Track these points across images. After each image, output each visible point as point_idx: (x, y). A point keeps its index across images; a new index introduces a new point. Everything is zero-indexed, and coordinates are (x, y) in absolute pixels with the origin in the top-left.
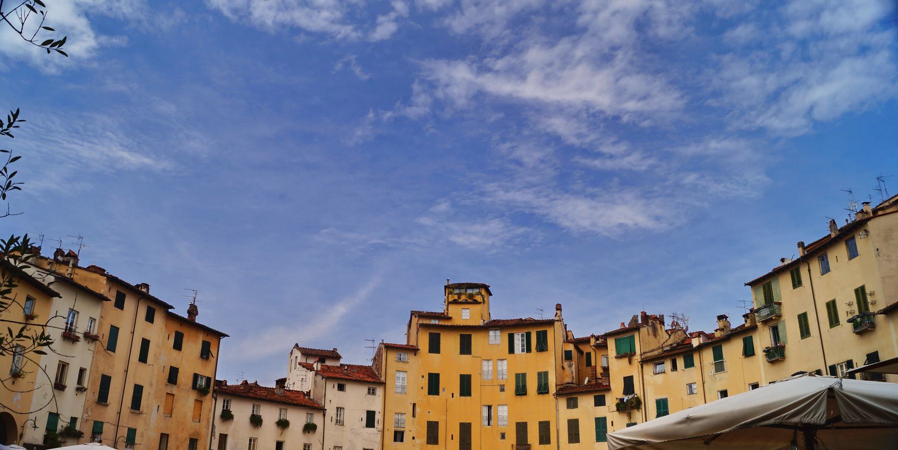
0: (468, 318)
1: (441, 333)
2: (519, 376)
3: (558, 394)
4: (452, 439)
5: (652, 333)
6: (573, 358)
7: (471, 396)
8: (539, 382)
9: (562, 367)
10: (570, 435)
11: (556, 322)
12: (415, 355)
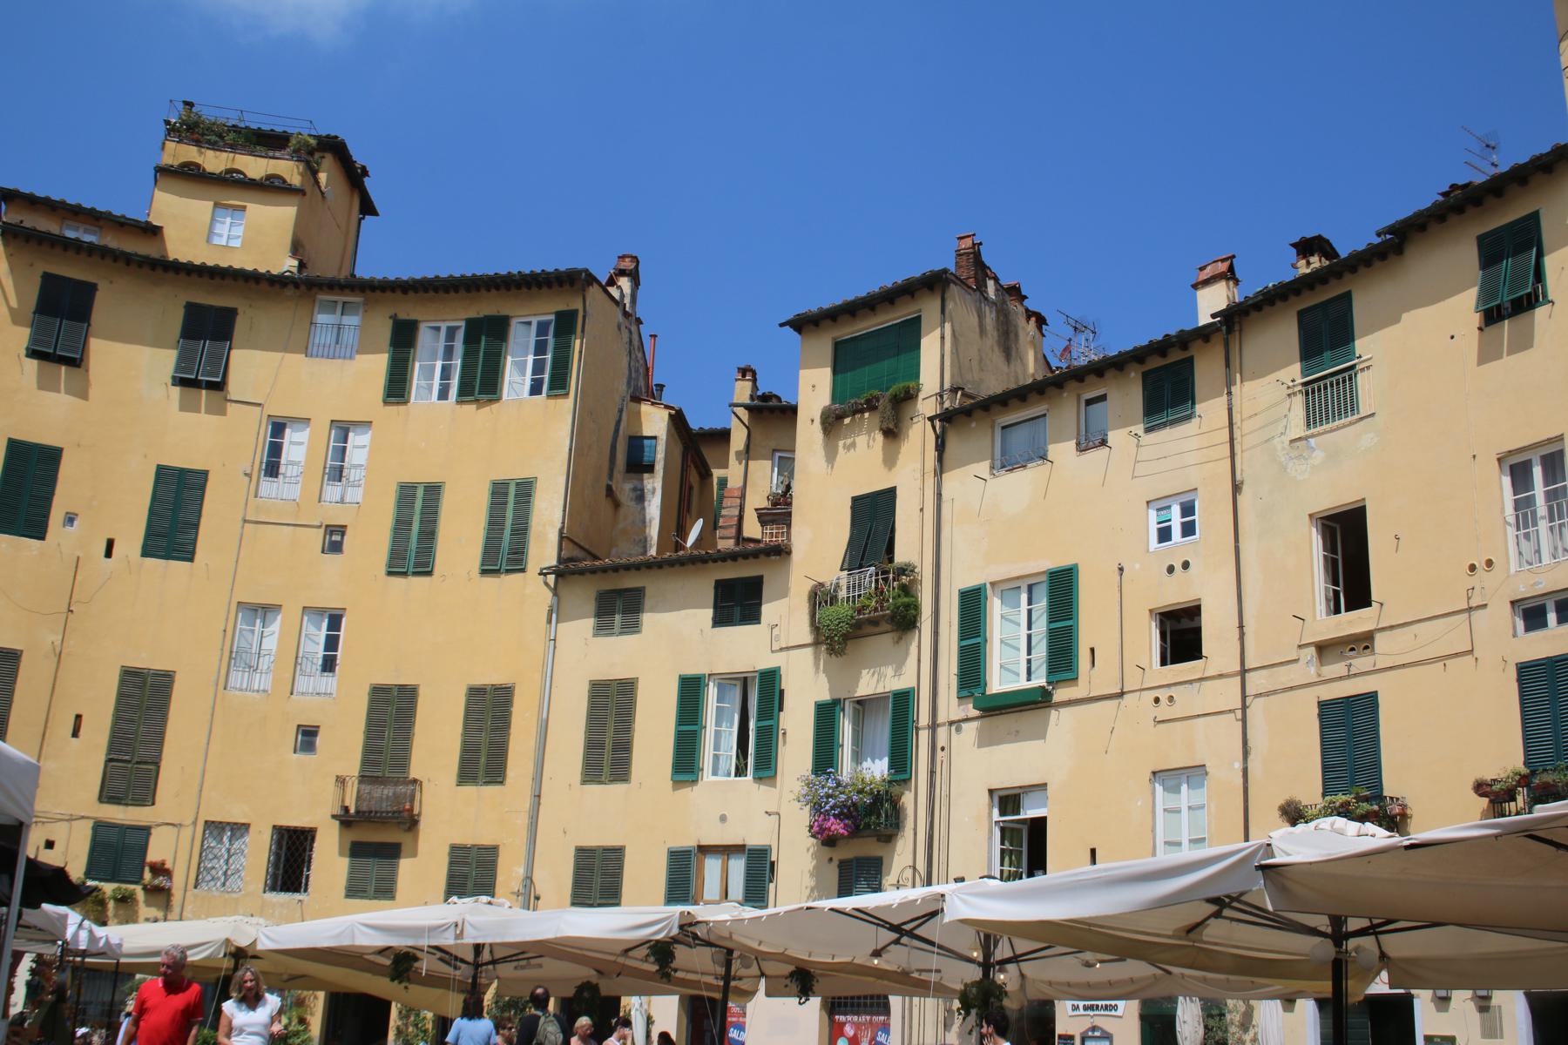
0: (236, 243)
1: (99, 287)
2: (414, 496)
3: (564, 572)
4: (75, 734)
5: (995, 334)
6: (659, 467)
7: (191, 560)
8: (490, 523)
9: (610, 492)
10: (593, 746)
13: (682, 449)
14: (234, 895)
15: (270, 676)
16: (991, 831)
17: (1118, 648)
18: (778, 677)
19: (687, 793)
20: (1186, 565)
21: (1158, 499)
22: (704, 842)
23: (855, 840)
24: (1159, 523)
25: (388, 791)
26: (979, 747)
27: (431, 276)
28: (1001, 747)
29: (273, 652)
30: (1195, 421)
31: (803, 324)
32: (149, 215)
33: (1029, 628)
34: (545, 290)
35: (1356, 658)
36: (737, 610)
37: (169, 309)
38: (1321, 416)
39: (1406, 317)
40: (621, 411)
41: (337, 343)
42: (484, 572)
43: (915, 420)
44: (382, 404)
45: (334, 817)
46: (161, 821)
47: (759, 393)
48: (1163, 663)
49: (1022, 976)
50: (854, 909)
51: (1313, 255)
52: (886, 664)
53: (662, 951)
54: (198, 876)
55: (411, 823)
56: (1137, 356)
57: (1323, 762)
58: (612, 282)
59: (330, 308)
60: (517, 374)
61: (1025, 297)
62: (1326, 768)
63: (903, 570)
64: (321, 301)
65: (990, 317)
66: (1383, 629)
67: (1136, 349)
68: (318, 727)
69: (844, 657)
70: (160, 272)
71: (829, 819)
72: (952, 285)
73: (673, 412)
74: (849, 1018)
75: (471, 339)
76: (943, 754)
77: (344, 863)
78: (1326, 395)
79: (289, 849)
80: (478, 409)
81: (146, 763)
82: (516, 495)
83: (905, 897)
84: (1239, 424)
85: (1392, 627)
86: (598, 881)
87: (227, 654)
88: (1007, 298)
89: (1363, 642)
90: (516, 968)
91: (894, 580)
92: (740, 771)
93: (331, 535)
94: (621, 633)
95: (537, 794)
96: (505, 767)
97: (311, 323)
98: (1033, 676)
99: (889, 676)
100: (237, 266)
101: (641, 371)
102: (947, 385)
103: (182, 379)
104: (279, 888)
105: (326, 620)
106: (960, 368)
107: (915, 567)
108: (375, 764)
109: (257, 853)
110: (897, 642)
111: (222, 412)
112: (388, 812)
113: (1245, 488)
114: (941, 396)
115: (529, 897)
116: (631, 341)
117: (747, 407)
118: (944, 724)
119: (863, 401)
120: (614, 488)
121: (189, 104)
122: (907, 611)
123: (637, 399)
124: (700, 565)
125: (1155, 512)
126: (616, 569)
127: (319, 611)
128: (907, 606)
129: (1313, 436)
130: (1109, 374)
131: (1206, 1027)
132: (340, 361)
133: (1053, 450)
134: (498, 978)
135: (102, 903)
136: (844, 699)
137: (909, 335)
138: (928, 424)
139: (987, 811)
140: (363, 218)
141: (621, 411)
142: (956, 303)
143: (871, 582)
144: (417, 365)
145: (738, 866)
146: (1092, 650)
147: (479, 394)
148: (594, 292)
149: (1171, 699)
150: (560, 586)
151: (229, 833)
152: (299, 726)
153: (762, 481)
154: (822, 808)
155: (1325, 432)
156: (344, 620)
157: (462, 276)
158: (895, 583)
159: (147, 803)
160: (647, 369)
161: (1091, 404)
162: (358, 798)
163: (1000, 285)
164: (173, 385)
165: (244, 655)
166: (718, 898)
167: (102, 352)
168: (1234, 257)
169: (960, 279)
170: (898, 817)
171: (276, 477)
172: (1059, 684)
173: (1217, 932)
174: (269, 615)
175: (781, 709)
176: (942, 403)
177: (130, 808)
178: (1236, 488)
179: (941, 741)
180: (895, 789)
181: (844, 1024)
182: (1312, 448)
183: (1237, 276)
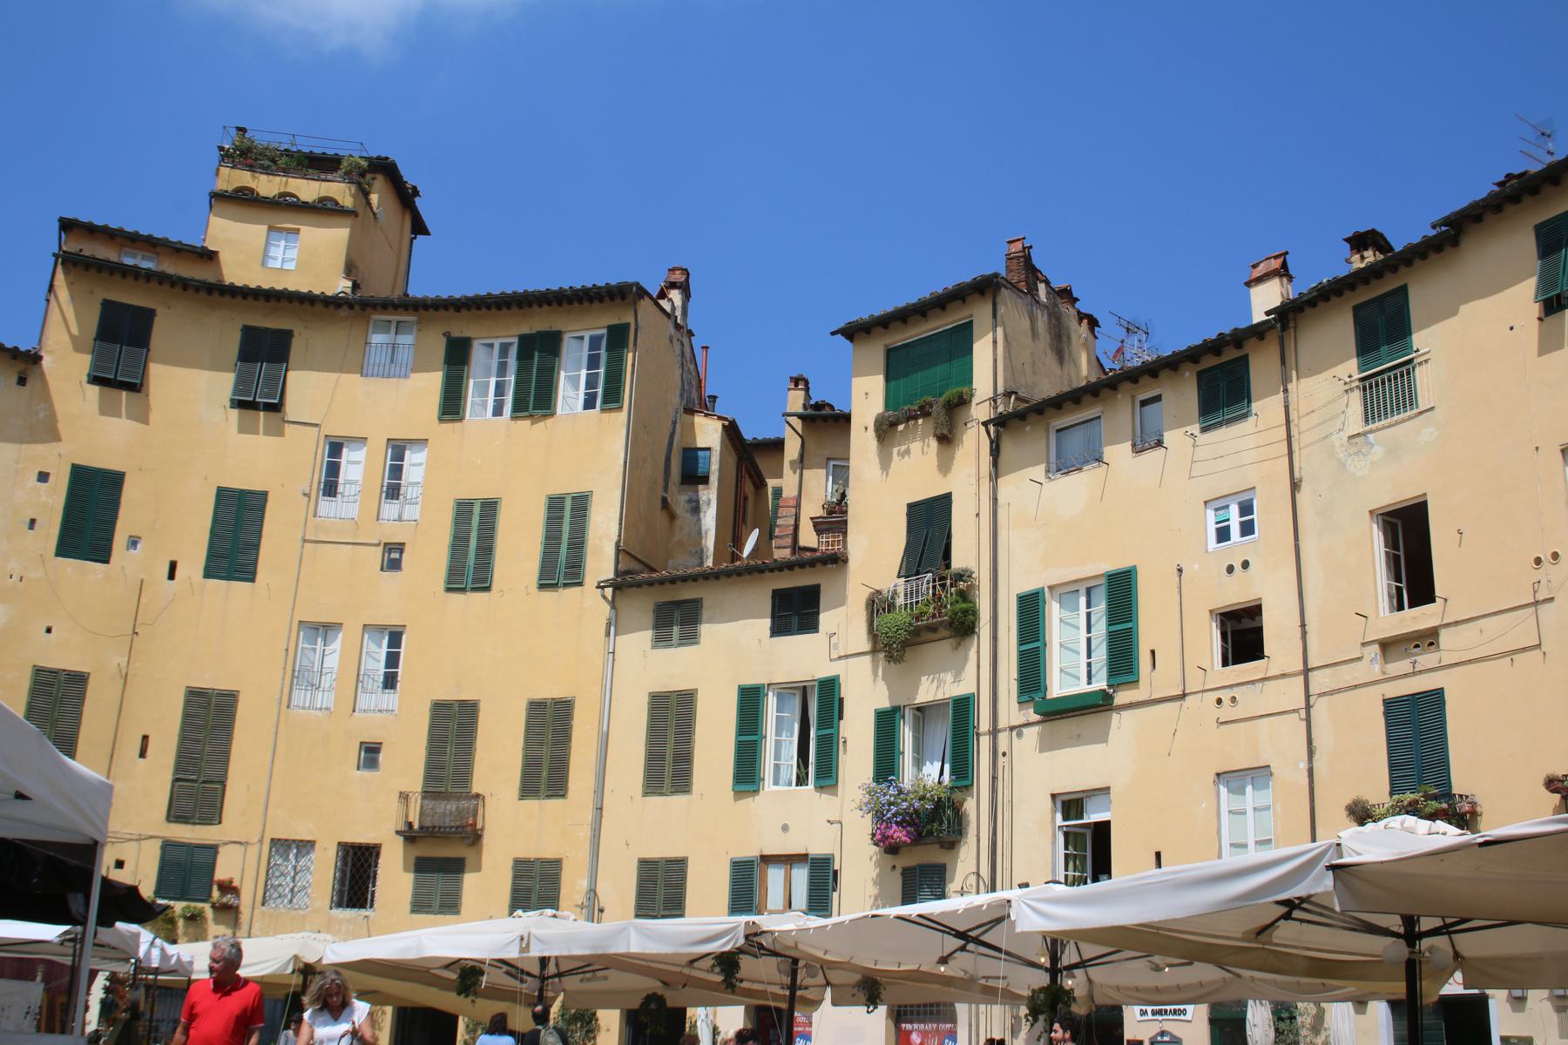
0: (291, 266)
1: (158, 312)
2: (471, 512)
3: (622, 585)
4: (143, 754)
5: (1048, 338)
7: (253, 580)
8: (548, 538)
11: (647, 299)
12: (22, 381)
13: (736, 459)
14: (301, 912)
15: (332, 694)
16: (1054, 836)
17: (1179, 649)
18: (837, 685)
19: (747, 802)
20: (1245, 565)
21: (1216, 499)
22: (767, 852)
23: (918, 847)
24: (1217, 523)
25: (451, 806)
26: (1040, 752)
27: (483, 293)
28: (1063, 751)
29: (336, 669)
30: (1251, 419)
31: (854, 332)
32: (204, 240)
33: (1089, 631)
34: (596, 304)
35: (1421, 654)
36: (795, 620)
37: (226, 333)
38: (1379, 411)
39: (1463, 309)
40: (674, 423)
41: (392, 361)
42: (542, 587)
43: (969, 425)
44: (437, 421)
45: (398, 832)
46: (228, 839)
47: (812, 402)
48: (1225, 663)
49: (1090, 980)
50: (920, 916)
51: (1366, 249)
52: (945, 670)
53: (727, 963)
54: (265, 893)
55: (474, 837)
56: (1191, 356)
57: (1390, 761)
58: (662, 295)
59: (384, 327)
60: (570, 390)
61: (1077, 300)
62: (1393, 767)
63: (961, 576)
64: (375, 321)
65: (1042, 320)
66: (1448, 625)
67: (1190, 349)
68: (381, 743)
69: (903, 663)
70: (216, 296)
71: (891, 827)
72: (1003, 290)
73: (727, 423)
74: (916, 1026)
75: (524, 355)
76: (1005, 759)
77: (408, 879)
78: (1384, 390)
79: (354, 865)
80: (532, 424)
81: (212, 782)
82: (572, 509)
83: (971, 903)
84: (1296, 422)
85: (1457, 623)
86: (661, 893)
87: (289, 673)
88: (1059, 300)
89: (1428, 639)
90: (581, 980)
91: (952, 586)
92: (801, 780)
93: (390, 553)
94: (679, 645)
95: (599, 806)
96: (567, 781)
97: (366, 343)
98: (1093, 680)
99: (948, 683)
100: (291, 288)
101: (694, 383)
102: (1000, 390)
103: (239, 401)
104: (345, 904)
105: (387, 637)
106: (1013, 372)
107: (972, 573)
108: (439, 779)
109: (322, 870)
110: (956, 649)
111: (281, 434)
112: (451, 827)
113: (1304, 485)
114: (995, 401)
115: (593, 909)
116: (683, 353)
117: (800, 416)
118: (1004, 730)
119: (916, 408)
120: (669, 499)
121: (242, 130)
122: (965, 616)
123: (690, 411)
124: (756, 574)
125: (1213, 512)
126: (673, 581)
127: (380, 629)
128: (965, 612)
129: (1371, 431)
130: (1164, 374)
131: (1277, 1030)
132: (395, 380)
133: (1109, 452)
134: (564, 990)
135: (172, 921)
136: (904, 706)
137: (961, 341)
138: (983, 428)
139: (1050, 816)
140: (415, 238)
141: (674, 423)
142: (1007, 307)
143: (928, 589)
144: (471, 382)
145: (801, 876)
146: (1153, 652)
147: (533, 409)
148: (645, 304)
149: (1233, 699)
150: (617, 599)
151: (295, 851)
152: (362, 743)
153: (816, 490)
154: (884, 816)
155: (1384, 428)
156: (404, 637)
157: (514, 293)
158: (953, 589)
159: (214, 822)
160: (700, 381)
161: (1147, 404)
162: (422, 814)
163: (1051, 288)
164: (231, 407)
165: (306, 674)
166: (781, 908)
167: (162, 377)
168: (1287, 253)
169: (1011, 284)
170: (960, 824)
171: (335, 496)
172: (1120, 687)
173: (1288, 934)
174: (330, 633)
175: (841, 717)
176: (996, 408)
177: (198, 827)
178: (1295, 486)
179: (1002, 746)
180: (957, 796)
181: (911, 1032)
182: (1371, 443)
183: (1291, 273)
